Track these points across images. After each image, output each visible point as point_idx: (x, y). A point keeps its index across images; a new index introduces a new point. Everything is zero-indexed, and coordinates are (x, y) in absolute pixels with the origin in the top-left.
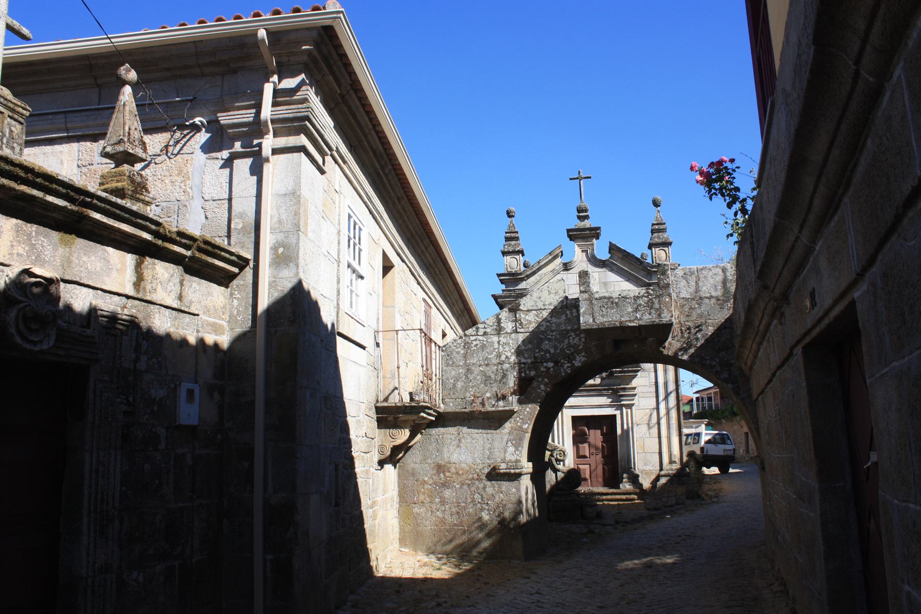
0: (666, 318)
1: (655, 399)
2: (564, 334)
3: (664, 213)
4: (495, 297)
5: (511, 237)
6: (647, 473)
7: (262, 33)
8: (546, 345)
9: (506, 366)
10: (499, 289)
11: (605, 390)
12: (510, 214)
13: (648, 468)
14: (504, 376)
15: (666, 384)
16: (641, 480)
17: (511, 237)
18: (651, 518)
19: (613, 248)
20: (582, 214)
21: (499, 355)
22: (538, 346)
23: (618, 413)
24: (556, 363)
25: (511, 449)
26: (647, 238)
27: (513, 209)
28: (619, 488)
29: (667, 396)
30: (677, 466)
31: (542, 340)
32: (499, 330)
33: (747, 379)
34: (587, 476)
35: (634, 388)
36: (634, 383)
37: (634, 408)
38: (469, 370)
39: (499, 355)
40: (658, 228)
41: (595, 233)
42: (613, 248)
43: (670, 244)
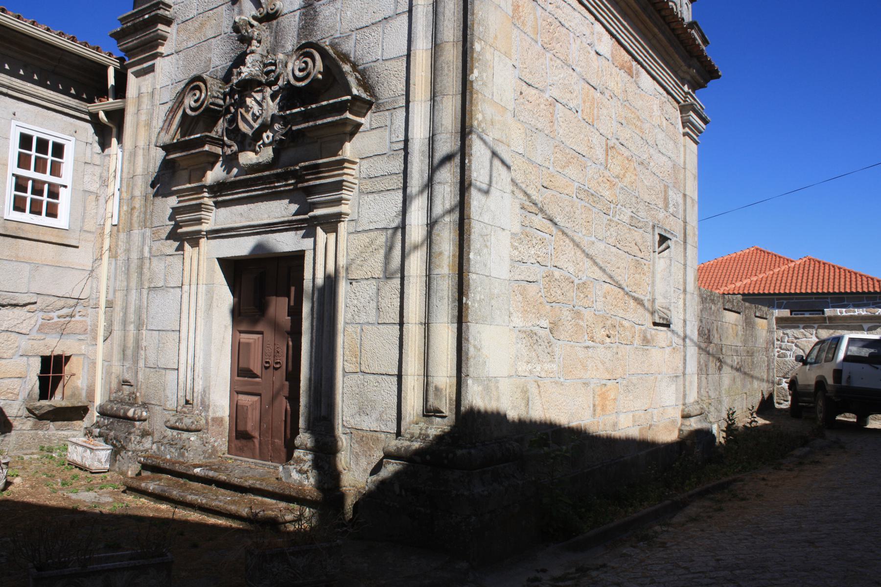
1: (399, 195)
6: (364, 438)
11: (279, 177)
13: (368, 423)
15: (432, 140)
16: (343, 460)
23: (308, 243)
29: (429, 185)
30: (437, 428)
34: (251, 426)
36: (349, 150)
37: (342, 227)
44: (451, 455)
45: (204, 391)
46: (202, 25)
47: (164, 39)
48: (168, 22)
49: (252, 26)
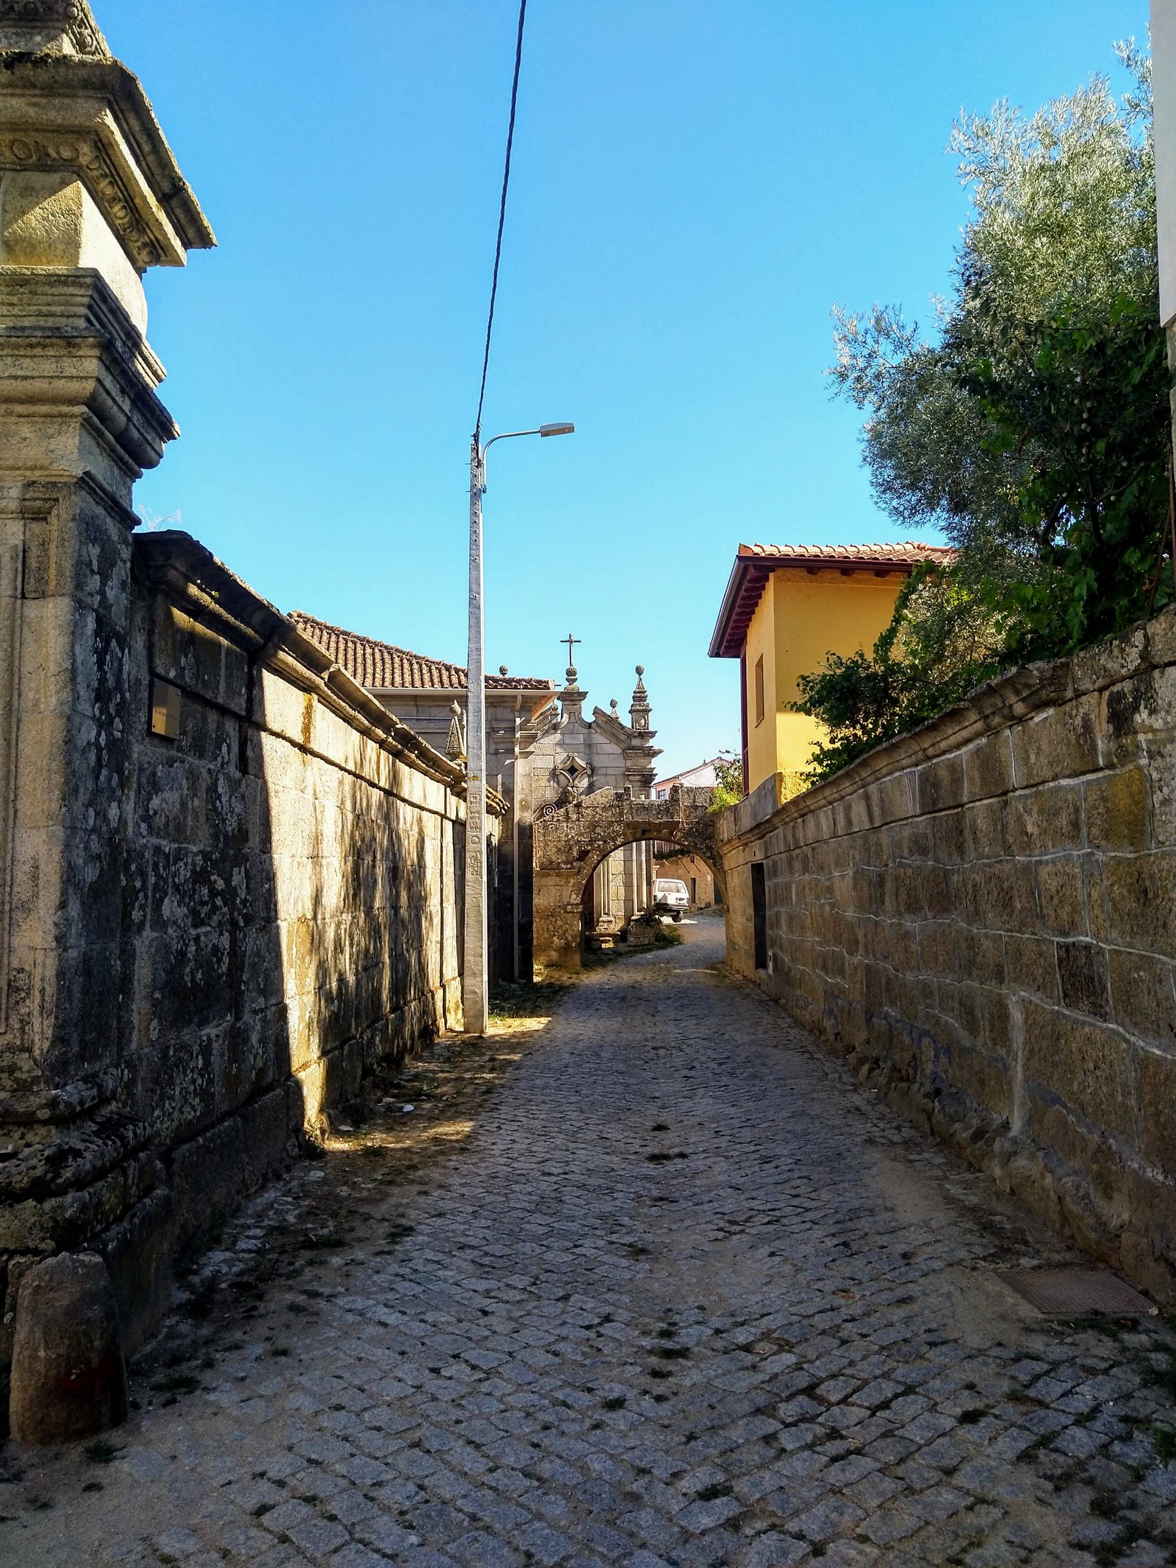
0: (676, 819)
2: (611, 824)
7: (520, 698)
8: (598, 830)
9: (571, 842)
14: (571, 849)
18: (636, 952)
19: (597, 711)
20: (571, 673)
21: (567, 835)
22: (593, 831)
24: (605, 842)
25: (574, 896)
31: (596, 827)
32: (567, 818)
33: (721, 858)
38: (546, 845)
39: (567, 835)
40: (640, 696)
41: (583, 695)
42: (597, 711)
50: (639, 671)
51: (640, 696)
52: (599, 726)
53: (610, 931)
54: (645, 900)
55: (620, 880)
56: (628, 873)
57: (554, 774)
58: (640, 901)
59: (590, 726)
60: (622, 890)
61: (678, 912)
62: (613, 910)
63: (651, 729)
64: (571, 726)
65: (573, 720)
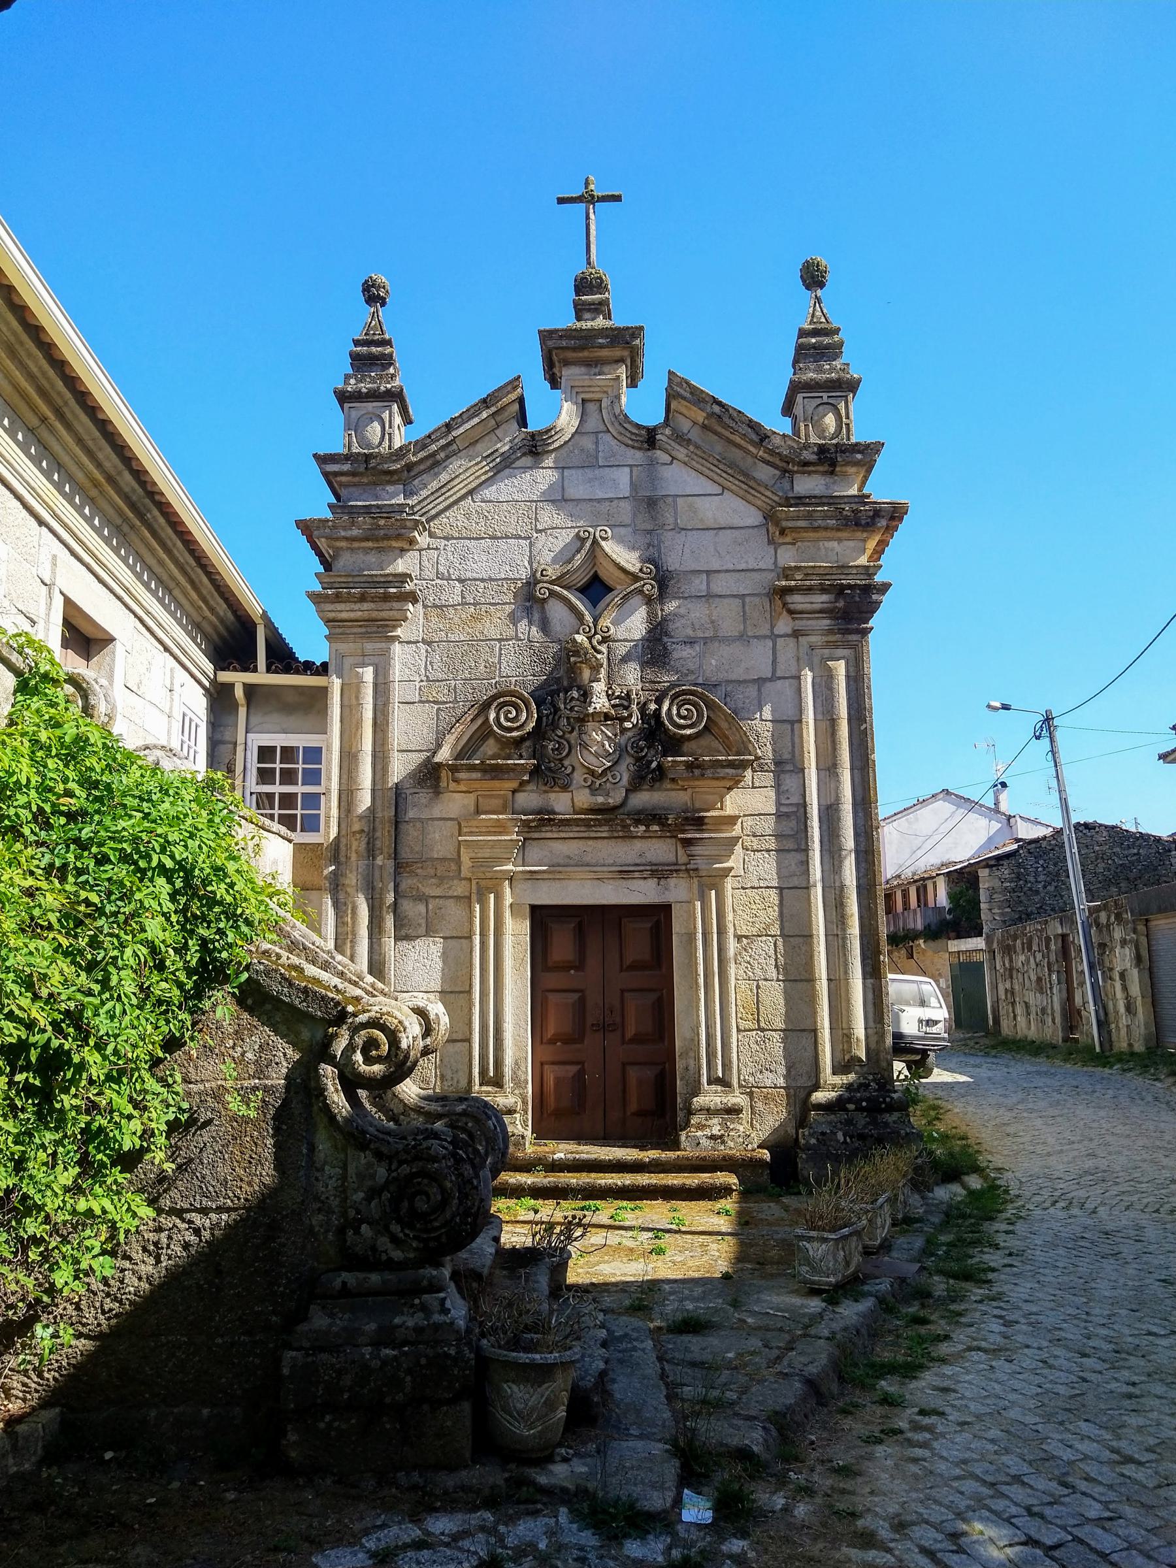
3: (837, 306)
4: (307, 528)
5: (371, 356)
10: (318, 502)
12: (373, 295)
17: (371, 356)
19: (679, 392)
26: (781, 374)
27: (382, 279)
28: (676, 1146)
35: (732, 820)
37: (729, 883)
40: (817, 345)
42: (679, 392)
43: (852, 386)
44: (888, 1100)
45: (516, 1063)
46: (475, 618)
47: (405, 619)
48: (413, 598)
49: (599, 652)
50: (813, 277)
51: (817, 345)
52: (681, 438)
53: (732, 1148)
54: (859, 1031)
55: (765, 956)
56: (795, 935)
57: (530, 599)
58: (842, 1034)
59: (649, 438)
60: (774, 996)
61: (924, 1053)
62: (743, 1066)
63: (857, 436)
64: (587, 443)
65: (593, 423)
